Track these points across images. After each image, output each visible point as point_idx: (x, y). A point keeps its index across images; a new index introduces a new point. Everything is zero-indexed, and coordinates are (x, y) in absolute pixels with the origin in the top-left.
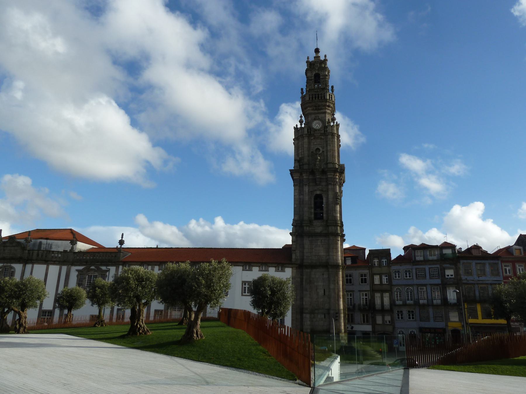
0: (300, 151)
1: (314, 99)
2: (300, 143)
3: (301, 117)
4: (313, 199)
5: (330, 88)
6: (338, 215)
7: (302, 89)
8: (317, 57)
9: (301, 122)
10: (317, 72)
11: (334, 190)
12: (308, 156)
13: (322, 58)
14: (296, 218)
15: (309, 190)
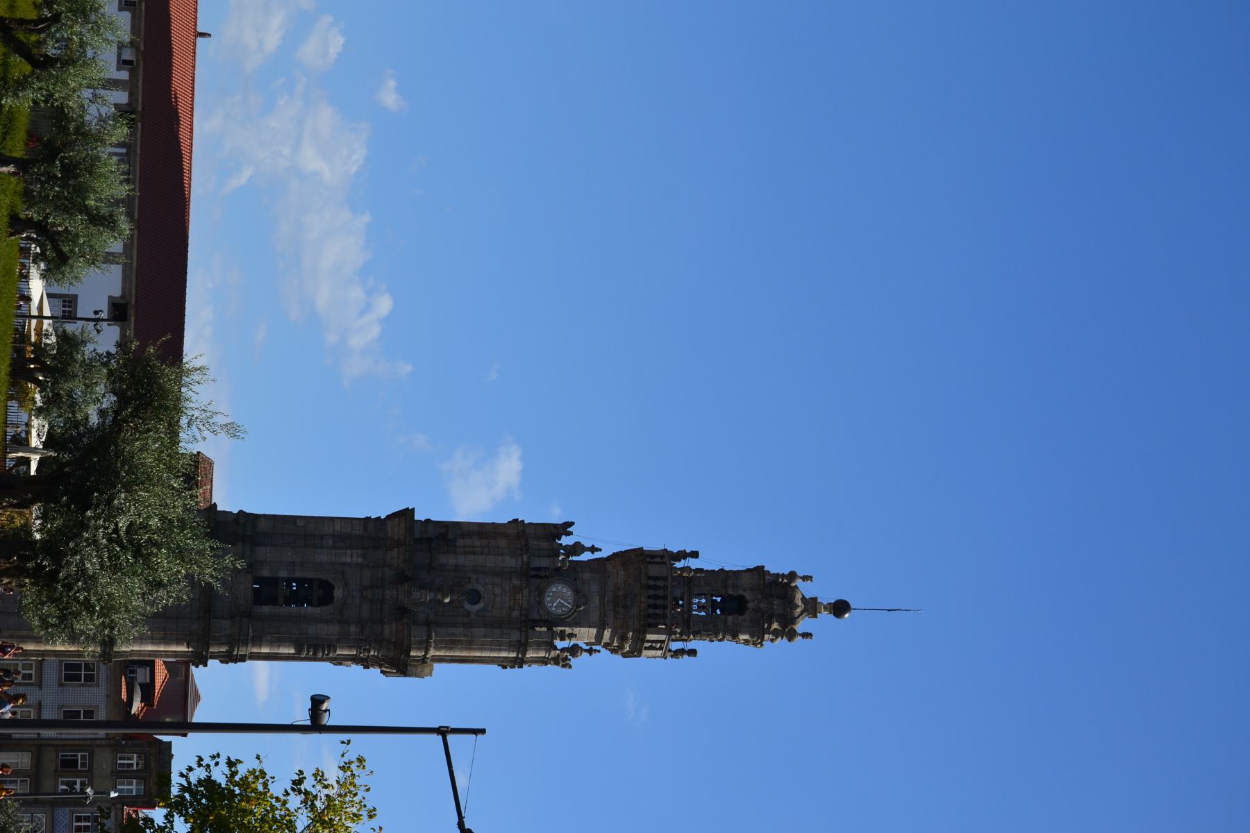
0: (477, 543)
1: (651, 592)
2: (503, 543)
3: (593, 549)
4: (319, 575)
5: (690, 645)
6: (265, 650)
7: (695, 555)
8: (812, 607)
9: (578, 548)
10: (751, 605)
11: (344, 640)
12: (457, 568)
13: (802, 625)
14: (262, 525)
15: (349, 565)
